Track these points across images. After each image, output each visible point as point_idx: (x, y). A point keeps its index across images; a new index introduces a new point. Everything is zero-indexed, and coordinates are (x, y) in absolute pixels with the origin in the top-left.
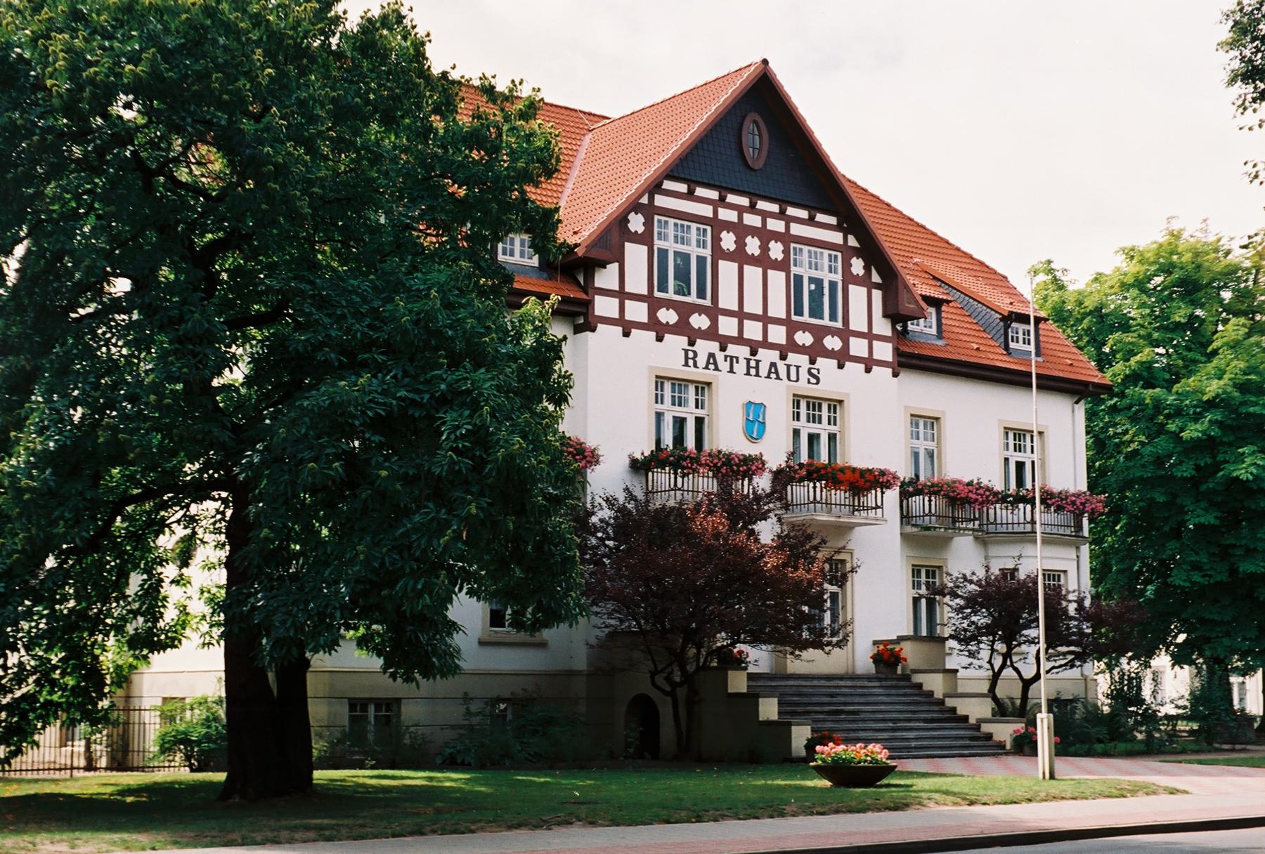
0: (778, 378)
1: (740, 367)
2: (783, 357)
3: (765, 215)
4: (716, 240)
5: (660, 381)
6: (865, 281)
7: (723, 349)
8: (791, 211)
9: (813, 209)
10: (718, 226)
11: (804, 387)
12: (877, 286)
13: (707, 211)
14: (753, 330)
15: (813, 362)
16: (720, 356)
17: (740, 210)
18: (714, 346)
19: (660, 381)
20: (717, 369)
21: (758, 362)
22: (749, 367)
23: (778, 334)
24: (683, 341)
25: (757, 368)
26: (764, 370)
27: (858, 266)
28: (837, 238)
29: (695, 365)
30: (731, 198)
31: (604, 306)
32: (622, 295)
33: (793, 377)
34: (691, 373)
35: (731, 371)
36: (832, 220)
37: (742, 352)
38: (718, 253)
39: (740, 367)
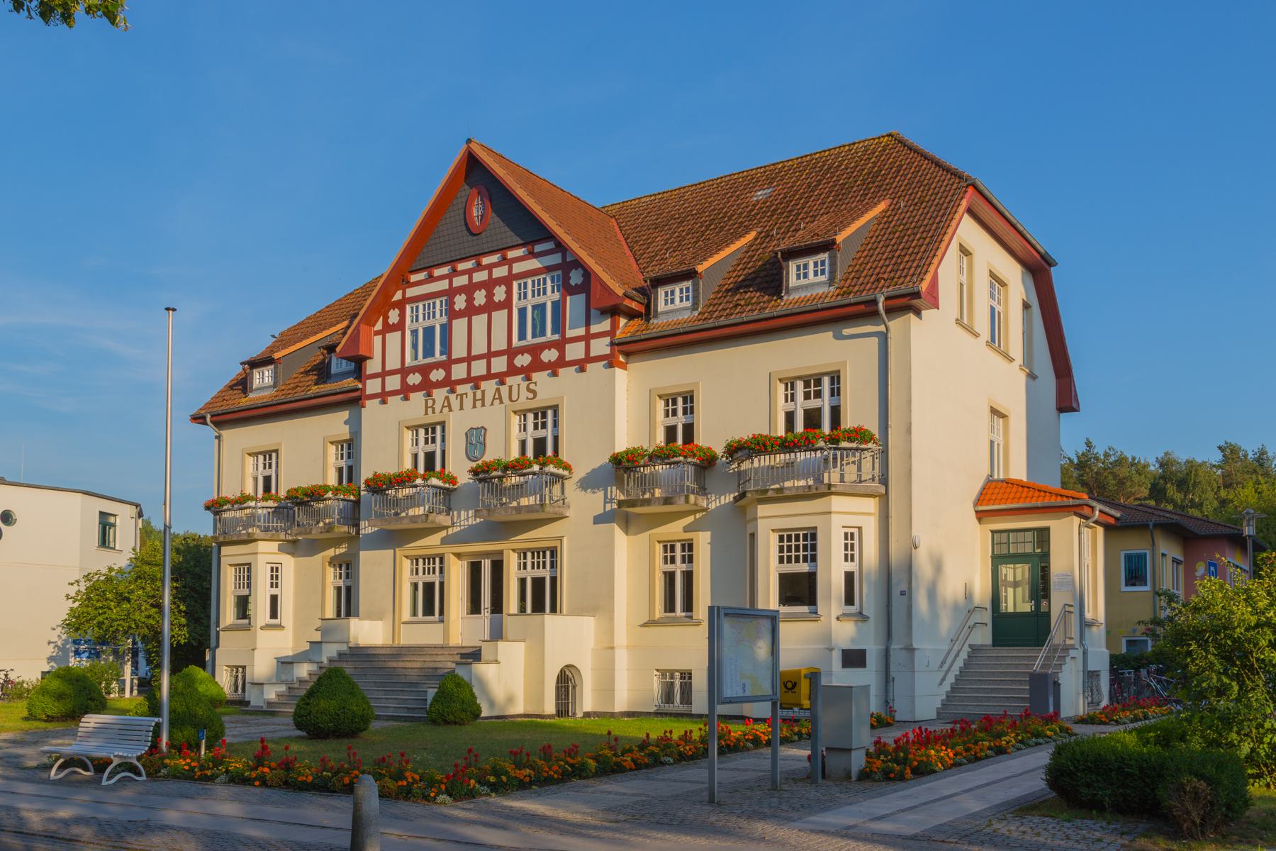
0: (501, 402)
1: (468, 402)
3: (490, 267)
11: (524, 401)
14: (479, 368)
17: (469, 272)
21: (483, 392)
25: (483, 399)
33: (514, 398)
34: (431, 418)
35: (461, 408)
38: (452, 314)
39: (468, 402)
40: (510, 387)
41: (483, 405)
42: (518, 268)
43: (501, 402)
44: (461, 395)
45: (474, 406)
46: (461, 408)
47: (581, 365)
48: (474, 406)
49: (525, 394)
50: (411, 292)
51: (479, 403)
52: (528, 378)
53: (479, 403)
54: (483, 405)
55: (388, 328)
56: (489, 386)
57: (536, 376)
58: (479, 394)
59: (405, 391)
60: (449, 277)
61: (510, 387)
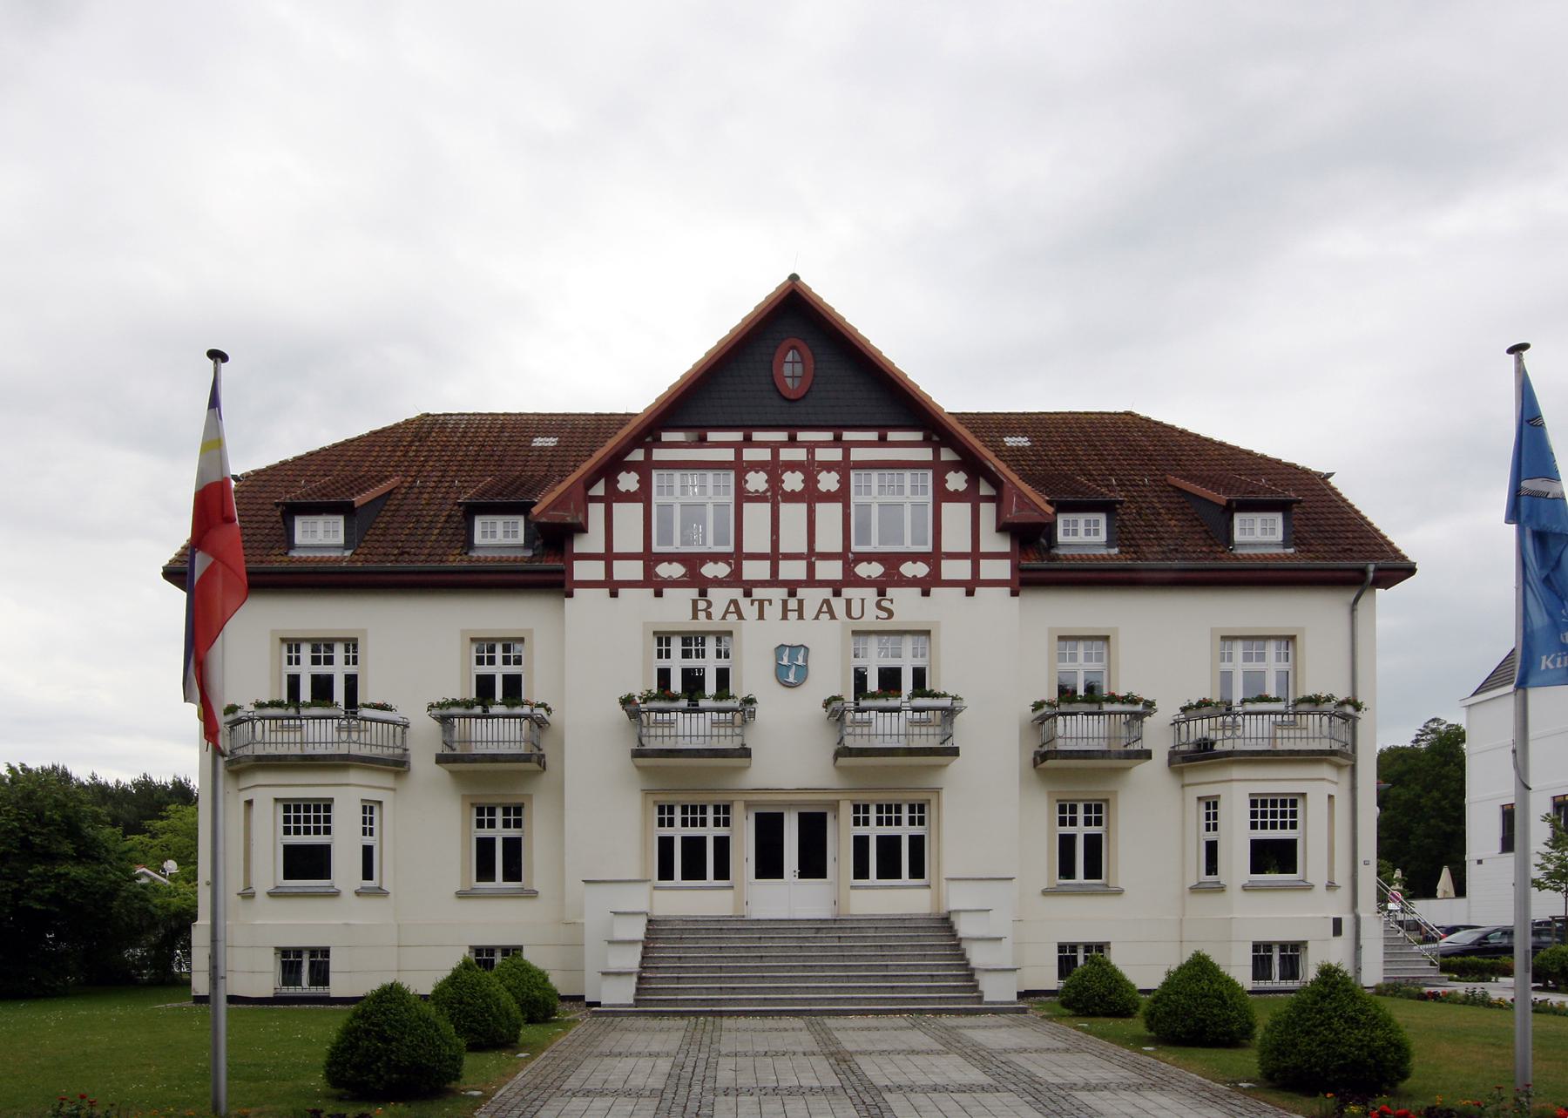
0: (833, 617)
2: (837, 594)
3: (811, 447)
5: (663, 639)
7: (748, 594)
8: (848, 436)
9: (883, 428)
11: (871, 617)
12: (988, 499)
13: (728, 455)
14: (792, 570)
15: (882, 593)
16: (744, 603)
17: (775, 447)
18: (737, 593)
19: (663, 639)
20: (741, 617)
21: (801, 602)
22: (785, 610)
24: (693, 593)
26: (810, 610)
27: (956, 481)
28: (926, 454)
29: (709, 616)
30: (758, 436)
31: (582, 570)
32: (609, 557)
33: (856, 612)
34: (702, 624)
35: (761, 617)
36: (917, 436)
37: (780, 593)
38: (742, 496)
40: (849, 602)
41: (801, 617)
42: (857, 454)
43: (833, 617)
44: (761, 602)
45: (785, 617)
46: (761, 617)
47: (970, 587)
48: (785, 617)
49: (872, 611)
50: (659, 454)
51: (793, 616)
52: (882, 593)
53: (793, 616)
54: (801, 617)
55: (614, 496)
56: (812, 597)
57: (891, 592)
58: (793, 604)
59: (658, 587)
60: (738, 447)
61: (849, 602)
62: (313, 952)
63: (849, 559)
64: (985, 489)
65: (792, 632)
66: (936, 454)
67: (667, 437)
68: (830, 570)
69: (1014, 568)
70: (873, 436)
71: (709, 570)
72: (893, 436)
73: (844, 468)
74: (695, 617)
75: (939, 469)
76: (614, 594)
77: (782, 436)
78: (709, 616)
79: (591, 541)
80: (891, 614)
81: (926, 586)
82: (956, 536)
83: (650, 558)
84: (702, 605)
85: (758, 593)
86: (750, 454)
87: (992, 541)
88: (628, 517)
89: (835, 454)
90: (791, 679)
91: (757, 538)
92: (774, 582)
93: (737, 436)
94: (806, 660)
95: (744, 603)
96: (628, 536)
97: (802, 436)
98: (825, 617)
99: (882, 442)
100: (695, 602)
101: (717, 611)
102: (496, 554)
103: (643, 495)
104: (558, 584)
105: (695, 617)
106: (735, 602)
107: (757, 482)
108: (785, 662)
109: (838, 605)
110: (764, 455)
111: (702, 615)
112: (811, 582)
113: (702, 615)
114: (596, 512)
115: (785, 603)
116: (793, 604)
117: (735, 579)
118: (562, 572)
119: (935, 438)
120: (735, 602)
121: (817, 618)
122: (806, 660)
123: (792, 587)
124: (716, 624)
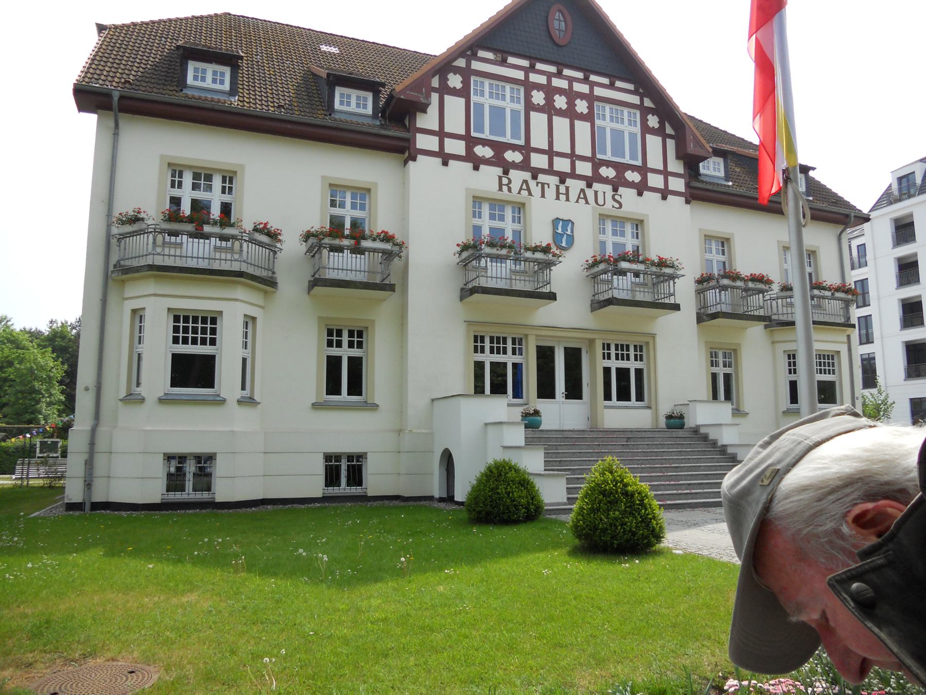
0: (587, 202)
1: (551, 192)
3: (571, 80)
4: (528, 97)
5: (478, 200)
6: (660, 131)
7: (534, 177)
8: (593, 78)
9: (613, 77)
10: (529, 87)
13: (520, 75)
14: (562, 165)
16: (532, 184)
17: (549, 76)
18: (527, 175)
19: (478, 200)
20: (530, 194)
21: (567, 188)
22: (558, 193)
23: (584, 168)
25: (567, 194)
26: (573, 195)
27: (653, 121)
28: (635, 100)
29: (510, 190)
30: (539, 66)
31: (424, 142)
32: (441, 134)
33: (601, 201)
34: (505, 194)
35: (543, 196)
36: (631, 87)
38: (530, 106)
39: (551, 192)
40: (596, 192)
41: (568, 199)
42: (598, 91)
43: (587, 202)
44: (543, 184)
45: (558, 198)
46: (543, 196)
47: (665, 193)
48: (558, 198)
49: (610, 202)
50: (476, 65)
51: (563, 197)
53: (563, 197)
54: (568, 199)
55: (445, 90)
56: (575, 186)
57: (622, 190)
58: (562, 189)
61: (596, 192)
62: (350, 457)
63: (597, 164)
64: (669, 130)
65: (564, 209)
66: (642, 101)
67: (482, 54)
68: (584, 168)
69: (687, 185)
70: (606, 81)
71: (510, 156)
72: (619, 84)
73: (591, 98)
74: (501, 189)
75: (645, 112)
76: (445, 164)
77: (580, 75)
78: (510, 190)
79: (428, 120)
80: (621, 206)
81: (641, 188)
82: (655, 162)
83: (471, 142)
84: (505, 181)
85: (542, 178)
86: (557, 82)
87: (676, 166)
88: (455, 106)
89: (584, 88)
90: (564, 244)
91: (539, 140)
92: (550, 171)
93: (552, 69)
94: (572, 232)
95: (532, 184)
96: (455, 123)
97: (567, 72)
98: (582, 201)
99: (611, 86)
100: (500, 178)
101: (515, 187)
102: (349, 118)
103: (464, 92)
104: (404, 151)
105: (501, 189)
106: (525, 182)
107: (538, 98)
108: (560, 231)
109: (590, 193)
110: (542, 80)
111: (505, 188)
112: (573, 175)
113: (505, 188)
114: (435, 97)
115: (558, 187)
116: (562, 189)
117: (525, 165)
118: (408, 140)
119: (641, 90)
120: (525, 182)
121: (577, 201)
122: (572, 232)
123: (563, 177)
124: (514, 196)
